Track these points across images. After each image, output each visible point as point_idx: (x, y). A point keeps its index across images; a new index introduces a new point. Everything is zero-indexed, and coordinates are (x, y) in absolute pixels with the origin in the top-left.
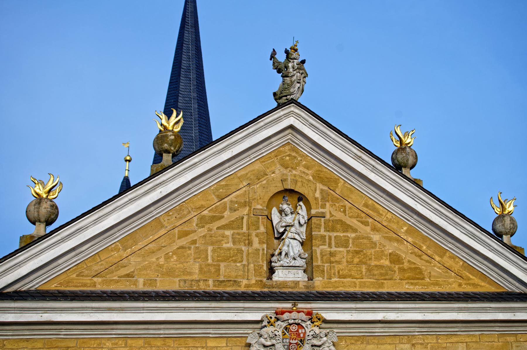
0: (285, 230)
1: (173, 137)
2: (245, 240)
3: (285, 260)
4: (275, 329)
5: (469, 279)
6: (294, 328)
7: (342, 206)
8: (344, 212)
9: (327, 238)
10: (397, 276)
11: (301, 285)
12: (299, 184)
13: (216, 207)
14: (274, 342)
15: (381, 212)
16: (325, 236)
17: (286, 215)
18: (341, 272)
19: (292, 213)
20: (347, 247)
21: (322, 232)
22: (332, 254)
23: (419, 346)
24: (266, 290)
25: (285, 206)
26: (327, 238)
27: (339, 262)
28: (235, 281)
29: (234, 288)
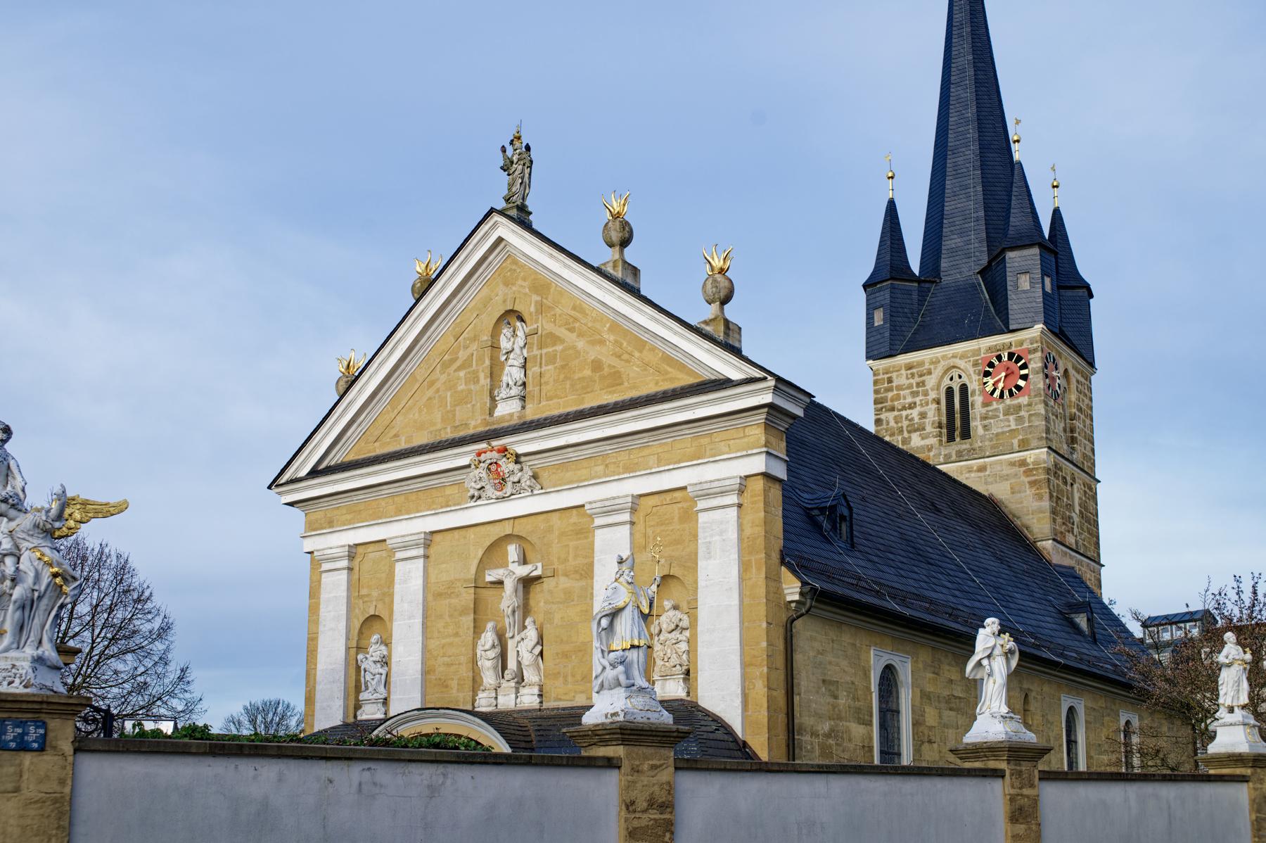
10: (597, 387)
23: (612, 466)
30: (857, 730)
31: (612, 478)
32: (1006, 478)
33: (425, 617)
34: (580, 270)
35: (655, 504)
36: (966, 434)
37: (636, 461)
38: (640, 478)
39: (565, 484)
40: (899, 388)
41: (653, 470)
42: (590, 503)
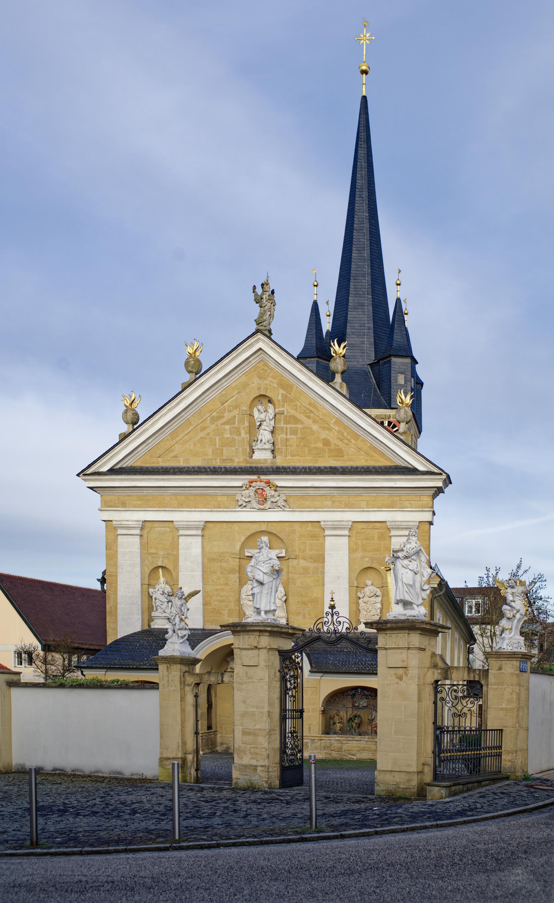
0: (261, 423)
1: (193, 362)
2: (237, 432)
3: (260, 445)
4: (250, 491)
5: (373, 456)
6: (260, 491)
7: (295, 405)
8: (296, 409)
9: (285, 428)
11: (269, 461)
12: (269, 390)
13: (220, 409)
14: (250, 499)
15: (319, 408)
16: (284, 427)
17: (262, 413)
18: (292, 453)
19: (265, 411)
20: (296, 435)
21: (282, 425)
22: (287, 440)
24: (249, 465)
25: (260, 407)
26: (285, 428)
27: (291, 446)
28: (231, 459)
29: (231, 464)
31: (338, 510)
33: (203, 572)
34: (322, 385)
35: (363, 528)
37: (353, 502)
38: (355, 512)
39: (306, 508)
41: (365, 510)
42: (324, 521)
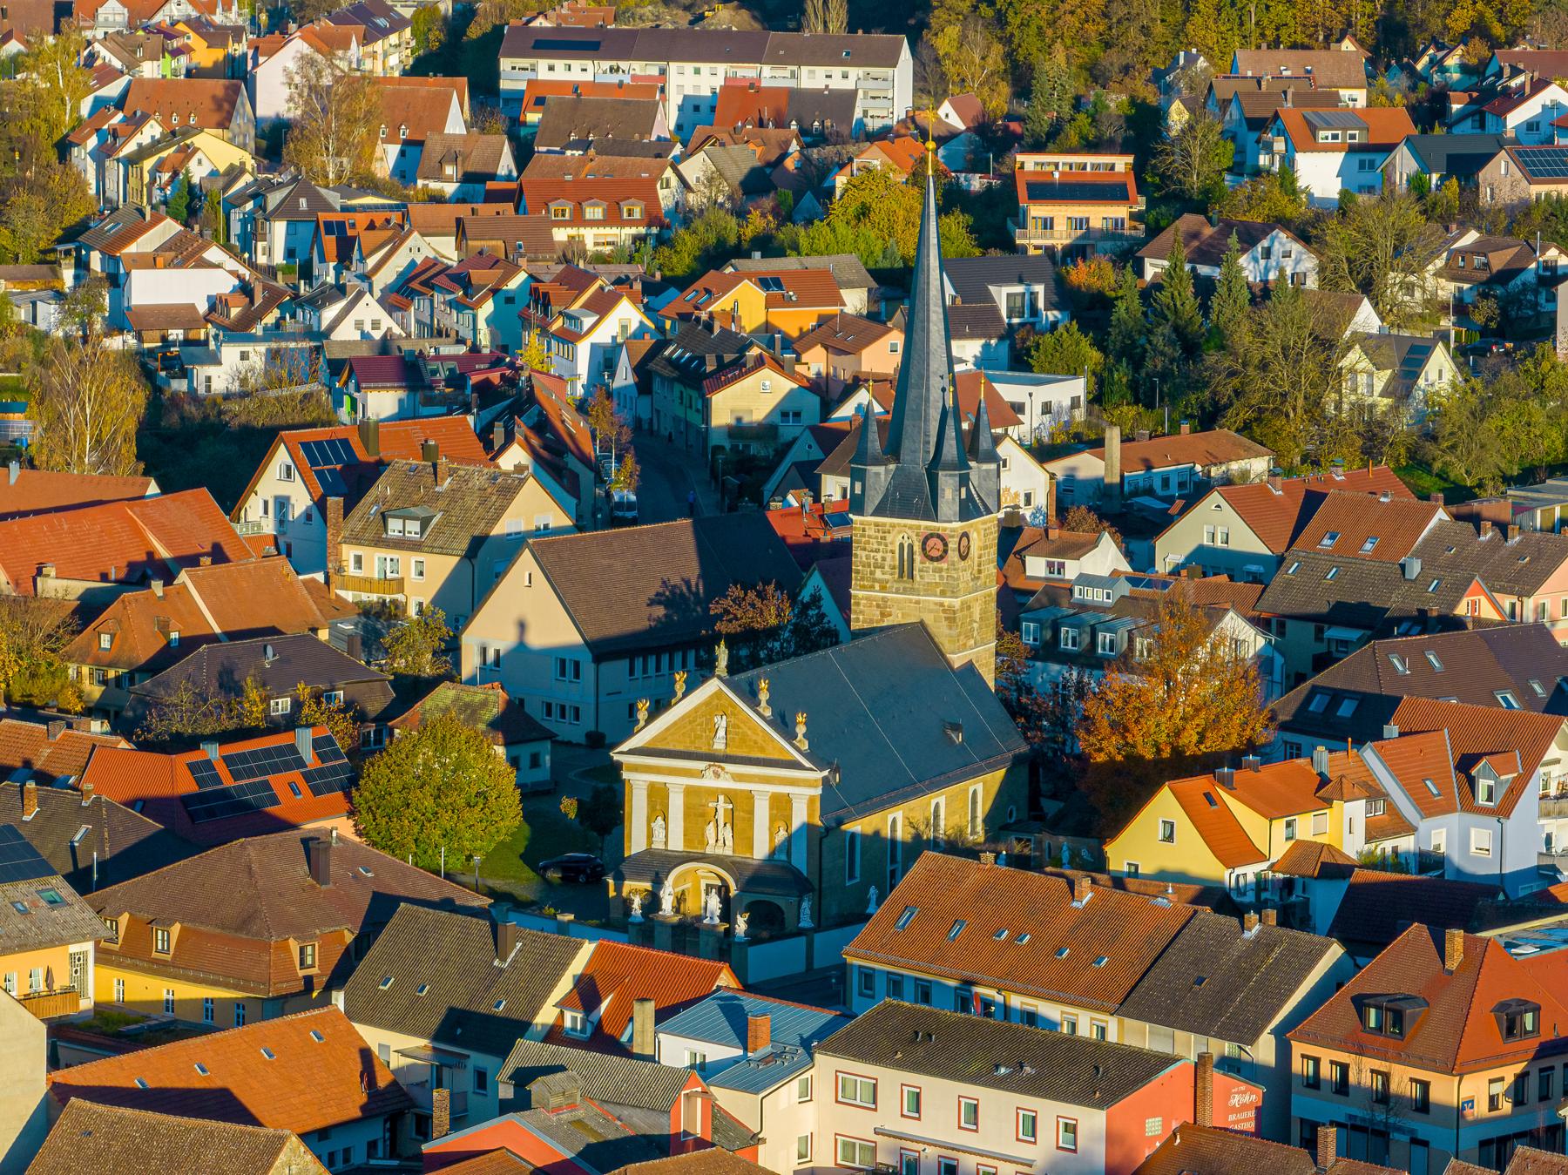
30: (841, 861)
32: (931, 611)
36: (911, 576)
40: (869, 537)
